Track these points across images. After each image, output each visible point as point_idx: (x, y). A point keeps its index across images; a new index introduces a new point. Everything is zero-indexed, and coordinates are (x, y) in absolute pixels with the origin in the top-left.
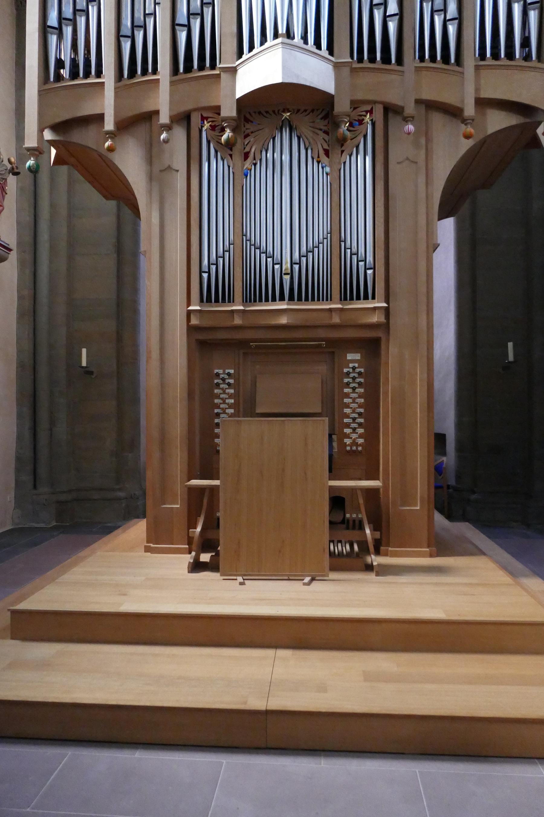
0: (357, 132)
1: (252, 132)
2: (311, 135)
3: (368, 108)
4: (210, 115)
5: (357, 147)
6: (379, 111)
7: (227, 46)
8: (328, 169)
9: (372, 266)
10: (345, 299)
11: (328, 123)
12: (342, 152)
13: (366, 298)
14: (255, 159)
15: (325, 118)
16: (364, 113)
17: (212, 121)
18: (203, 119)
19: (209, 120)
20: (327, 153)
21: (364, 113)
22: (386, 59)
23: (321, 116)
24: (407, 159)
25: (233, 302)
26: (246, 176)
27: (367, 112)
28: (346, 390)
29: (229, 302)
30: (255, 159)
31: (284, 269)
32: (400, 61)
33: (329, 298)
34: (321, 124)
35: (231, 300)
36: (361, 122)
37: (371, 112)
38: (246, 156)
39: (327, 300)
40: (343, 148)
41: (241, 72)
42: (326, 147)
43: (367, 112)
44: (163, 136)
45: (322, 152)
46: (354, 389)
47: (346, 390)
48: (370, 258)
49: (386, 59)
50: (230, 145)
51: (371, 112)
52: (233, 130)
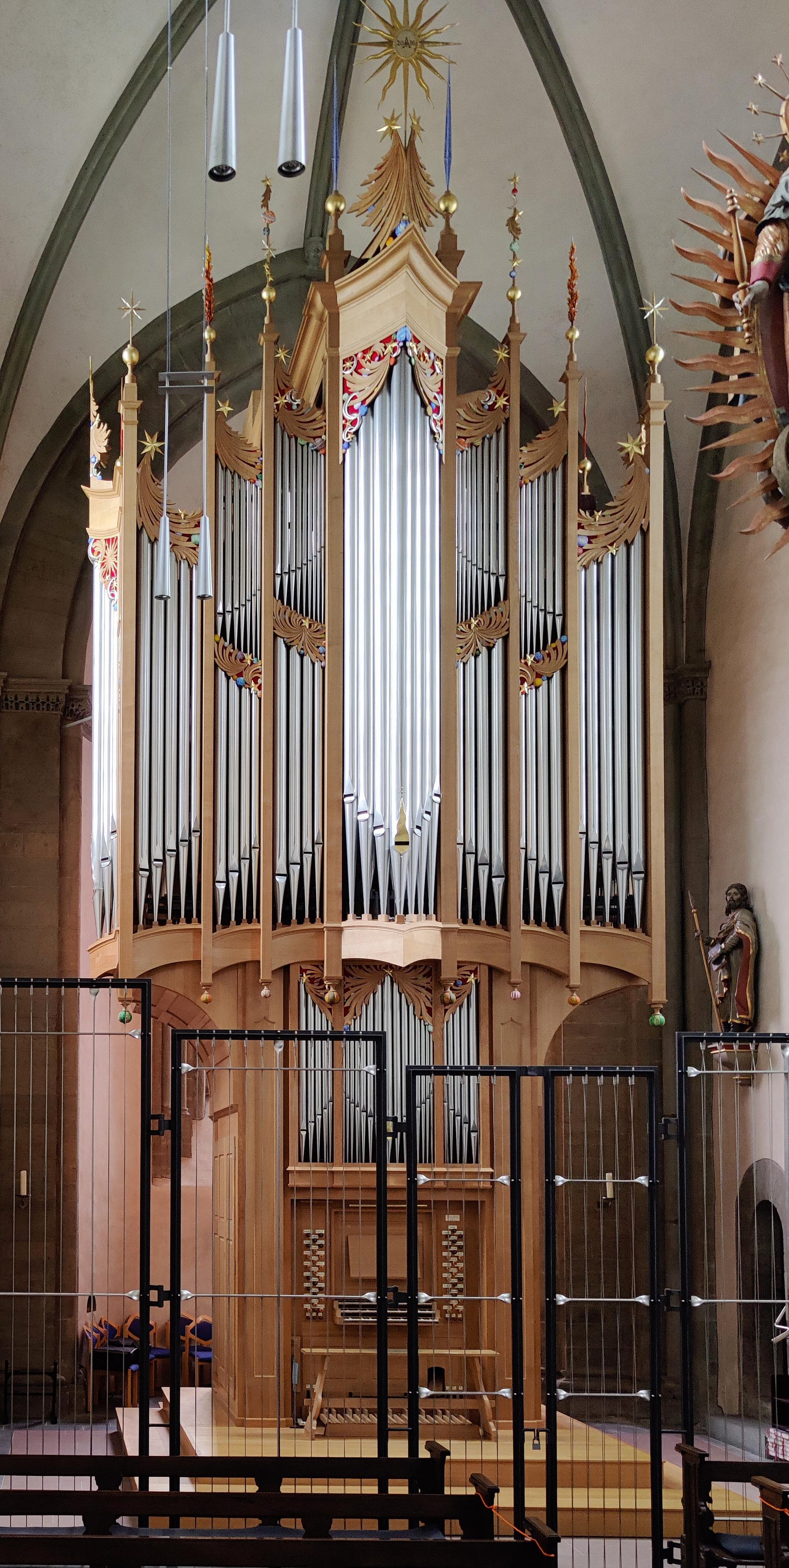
1: (352, 987)
2: (414, 991)
3: (473, 968)
4: (309, 967)
7: (331, 904)
8: (431, 1028)
12: (446, 1011)
13: (470, 1160)
14: (355, 1015)
15: (427, 975)
16: (468, 973)
17: (311, 974)
18: (302, 971)
19: (308, 972)
20: (430, 1011)
21: (468, 973)
23: (423, 973)
24: (512, 1020)
27: (471, 972)
28: (445, 1254)
34: (424, 981)
36: (464, 982)
38: (347, 1011)
39: (430, 1162)
40: (447, 1007)
41: (346, 933)
42: (429, 1005)
43: (471, 972)
44: (265, 992)
45: (425, 1011)
46: (454, 1252)
47: (445, 1254)
50: (332, 1002)
51: (475, 972)
52: (336, 988)
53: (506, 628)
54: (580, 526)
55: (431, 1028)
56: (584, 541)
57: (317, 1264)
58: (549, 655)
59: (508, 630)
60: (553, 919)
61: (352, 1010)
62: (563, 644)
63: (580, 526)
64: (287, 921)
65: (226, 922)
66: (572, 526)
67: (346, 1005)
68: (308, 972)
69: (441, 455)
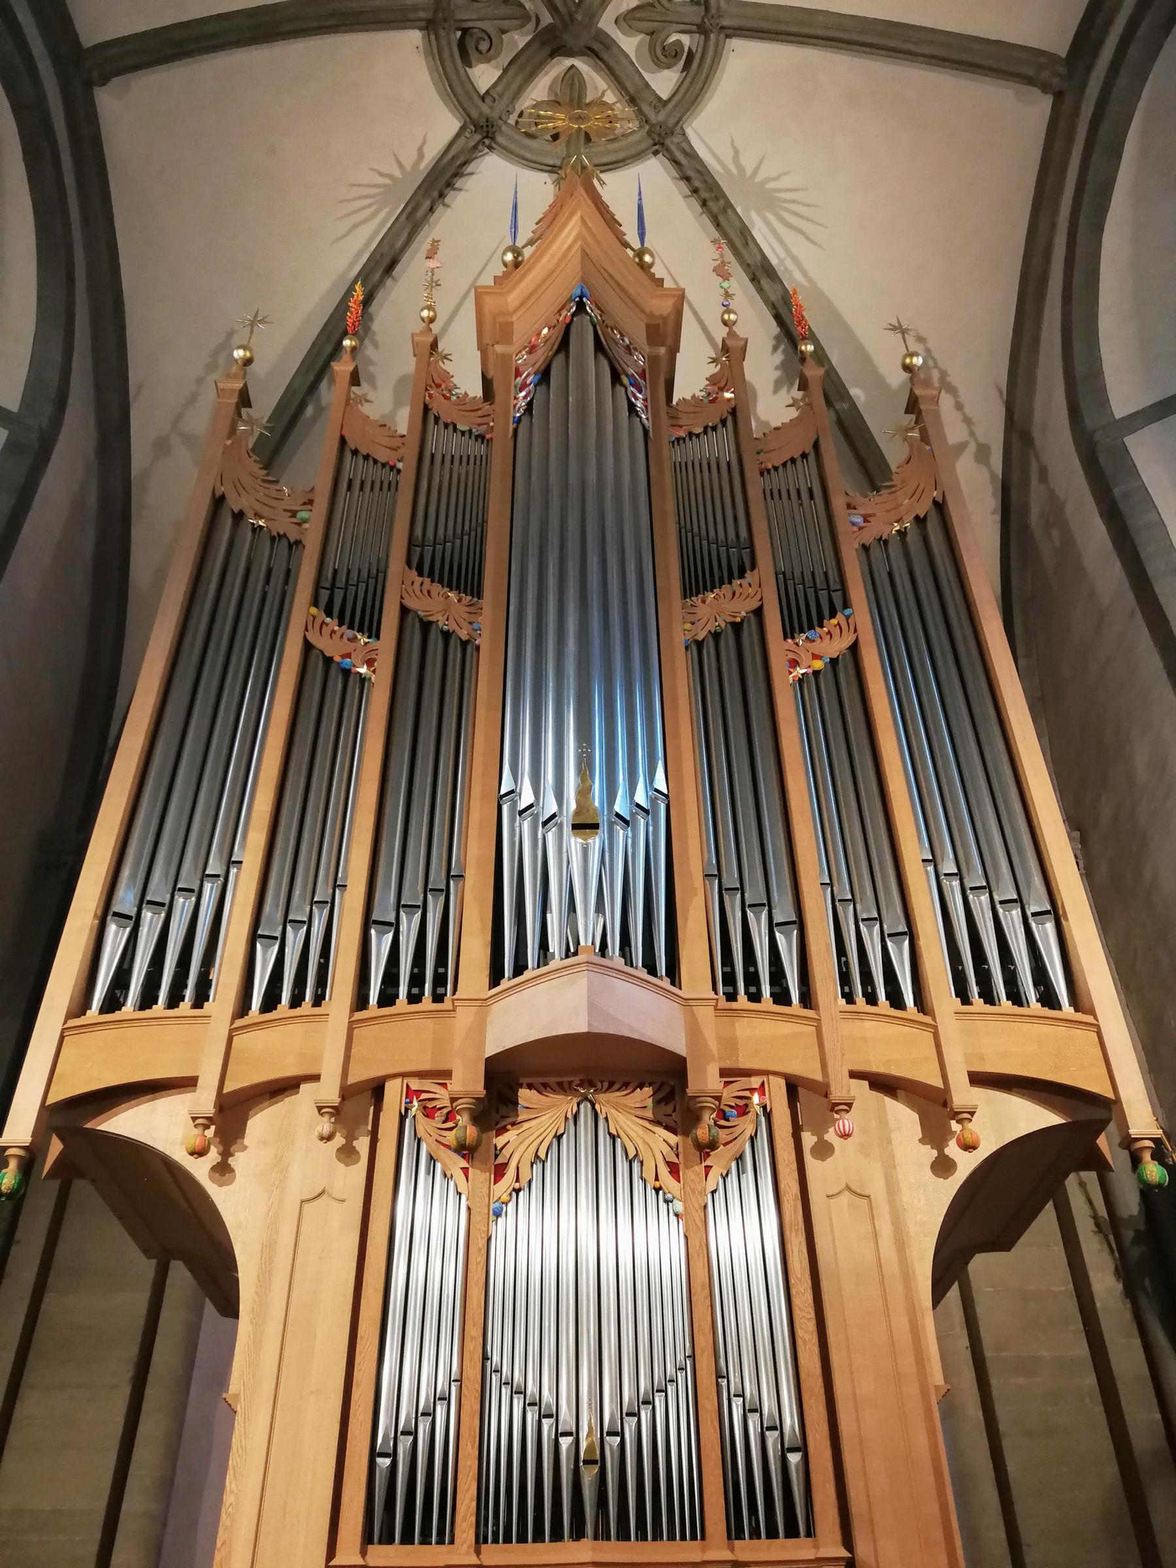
0: (737, 1131)
2: (640, 1131)
5: (740, 1159)
6: (778, 1087)
9: (800, 1443)
10: (740, 1535)
11: (674, 1110)
12: (708, 1168)
14: (517, 1180)
16: (747, 1094)
19: (424, 1096)
20: (674, 1170)
24: (848, 1188)
25: (452, 1542)
26: (498, 1214)
29: (441, 1542)
30: (517, 1180)
31: (583, 1445)
32: (807, 1000)
33: (697, 1532)
35: (445, 1536)
36: (743, 1111)
37: (761, 1089)
40: (708, 1163)
43: (752, 1090)
45: (664, 1171)
48: (790, 1420)
51: (761, 1089)
53: (758, 597)
55: (678, 1206)
56: (859, 520)
58: (829, 633)
59: (761, 599)
61: (510, 1173)
62: (848, 618)
64: (387, 999)
67: (500, 1160)
68: (424, 1096)
69: (646, 432)
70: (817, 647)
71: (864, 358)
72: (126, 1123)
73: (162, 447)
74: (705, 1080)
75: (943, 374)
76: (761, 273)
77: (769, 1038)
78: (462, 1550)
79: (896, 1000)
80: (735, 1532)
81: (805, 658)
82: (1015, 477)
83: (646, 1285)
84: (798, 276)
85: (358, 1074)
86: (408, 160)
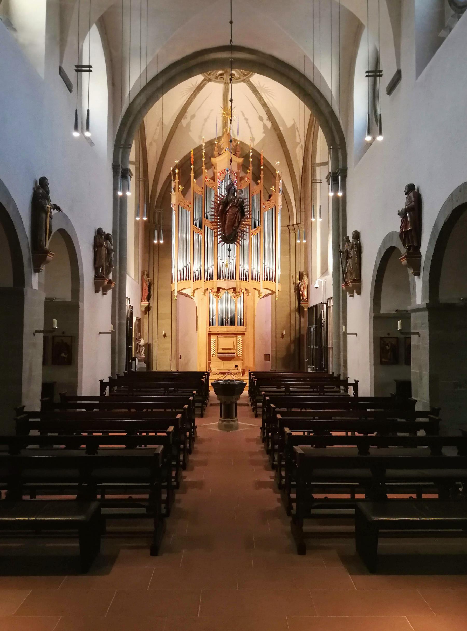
22: (246, 280)
49: (246, 280)
54: (263, 204)
56: (264, 207)
57: (213, 345)
60: (258, 279)
63: (263, 204)
64: (207, 280)
65: (196, 280)
66: (262, 204)
70: (255, 231)
71: (283, 121)
72: (183, 291)
73: (151, 144)
74: (238, 290)
75: (297, 128)
76: (264, 105)
77: (244, 284)
78: (217, 326)
79: (257, 280)
80: (238, 325)
81: (254, 233)
82: (305, 156)
83: (232, 310)
84: (271, 105)
85: (206, 288)
86: (194, 84)
